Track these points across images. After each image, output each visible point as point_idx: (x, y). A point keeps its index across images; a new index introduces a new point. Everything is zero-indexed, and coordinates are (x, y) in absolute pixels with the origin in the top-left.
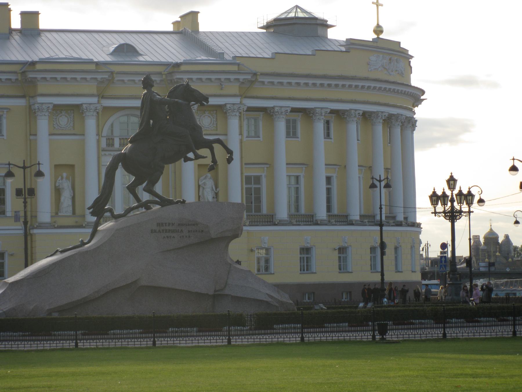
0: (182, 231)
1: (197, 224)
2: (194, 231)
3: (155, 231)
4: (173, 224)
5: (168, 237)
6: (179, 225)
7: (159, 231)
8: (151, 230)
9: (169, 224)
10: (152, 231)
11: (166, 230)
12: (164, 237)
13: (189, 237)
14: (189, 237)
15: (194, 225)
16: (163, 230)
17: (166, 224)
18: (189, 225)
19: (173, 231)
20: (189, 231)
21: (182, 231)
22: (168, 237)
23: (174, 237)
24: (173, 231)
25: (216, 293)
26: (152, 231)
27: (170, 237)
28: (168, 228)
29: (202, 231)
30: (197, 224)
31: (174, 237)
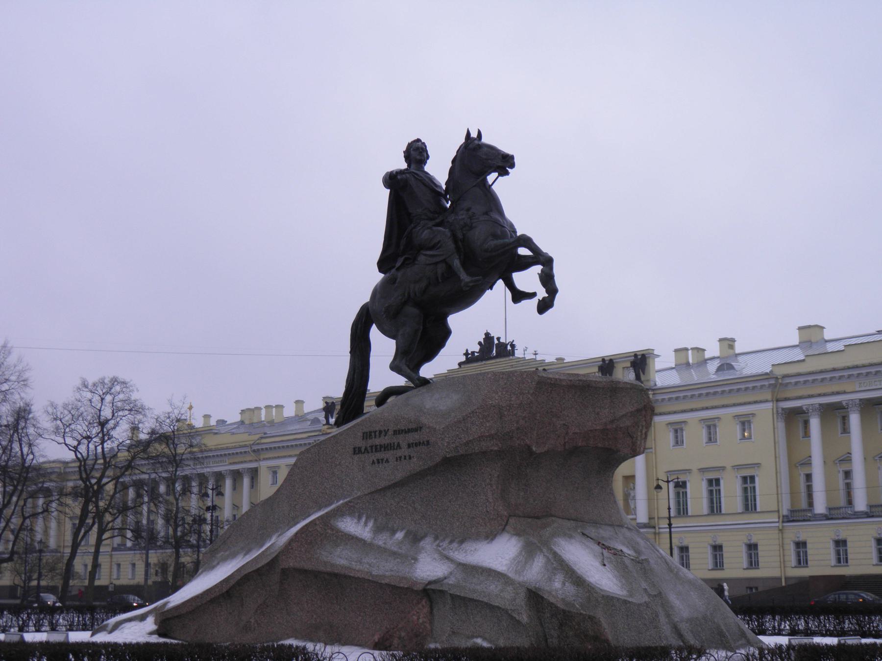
2: (416, 445)
4: (386, 432)
5: (379, 462)
6: (396, 432)
7: (366, 449)
8: (354, 448)
9: (380, 432)
10: (357, 451)
11: (376, 446)
12: (373, 462)
14: (410, 458)
15: (416, 430)
16: (372, 447)
17: (375, 432)
18: (409, 431)
20: (409, 446)
21: (399, 445)
23: (387, 461)
25: (428, 587)
26: (357, 451)
27: (382, 460)
28: (377, 441)
31: (387, 461)
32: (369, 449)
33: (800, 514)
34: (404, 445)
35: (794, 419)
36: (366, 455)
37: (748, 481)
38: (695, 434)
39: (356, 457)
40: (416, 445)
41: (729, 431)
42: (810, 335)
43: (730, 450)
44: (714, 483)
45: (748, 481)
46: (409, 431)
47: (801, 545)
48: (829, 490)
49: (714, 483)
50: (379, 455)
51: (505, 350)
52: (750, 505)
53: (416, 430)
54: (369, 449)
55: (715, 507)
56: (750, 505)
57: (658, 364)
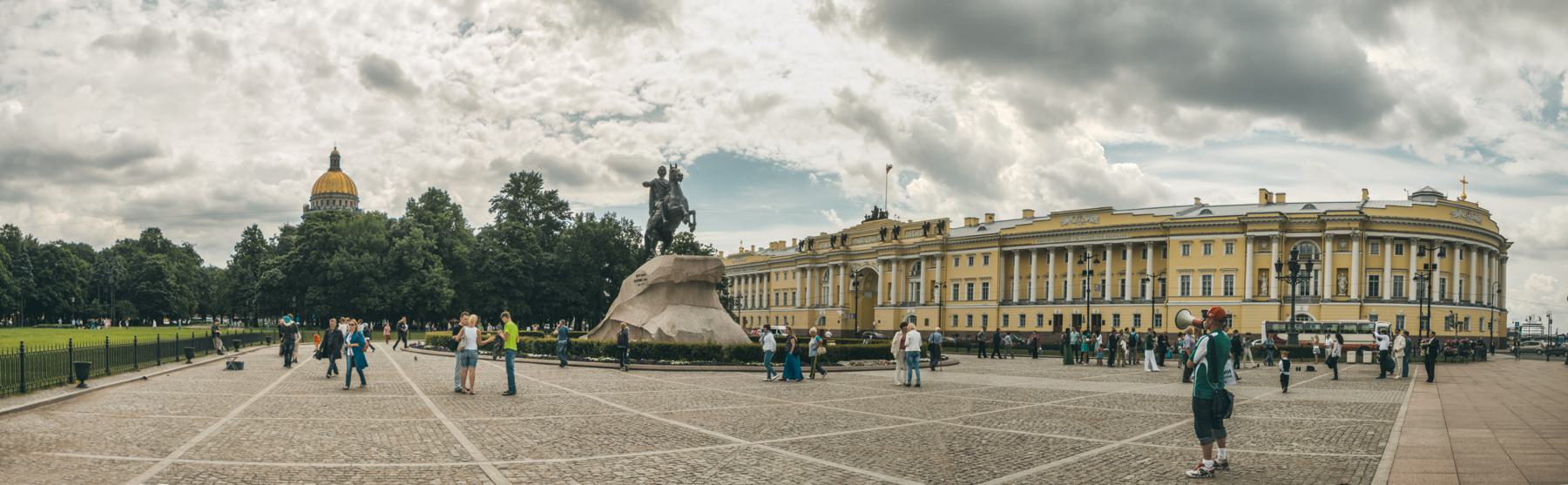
33: (1006, 301)
35: (1008, 256)
37: (986, 285)
38: (964, 261)
41: (979, 260)
42: (1028, 213)
43: (979, 271)
44: (971, 285)
45: (986, 285)
47: (1006, 316)
48: (1038, 288)
49: (971, 285)
51: (884, 215)
52: (985, 297)
55: (970, 298)
56: (985, 297)
57: (952, 226)
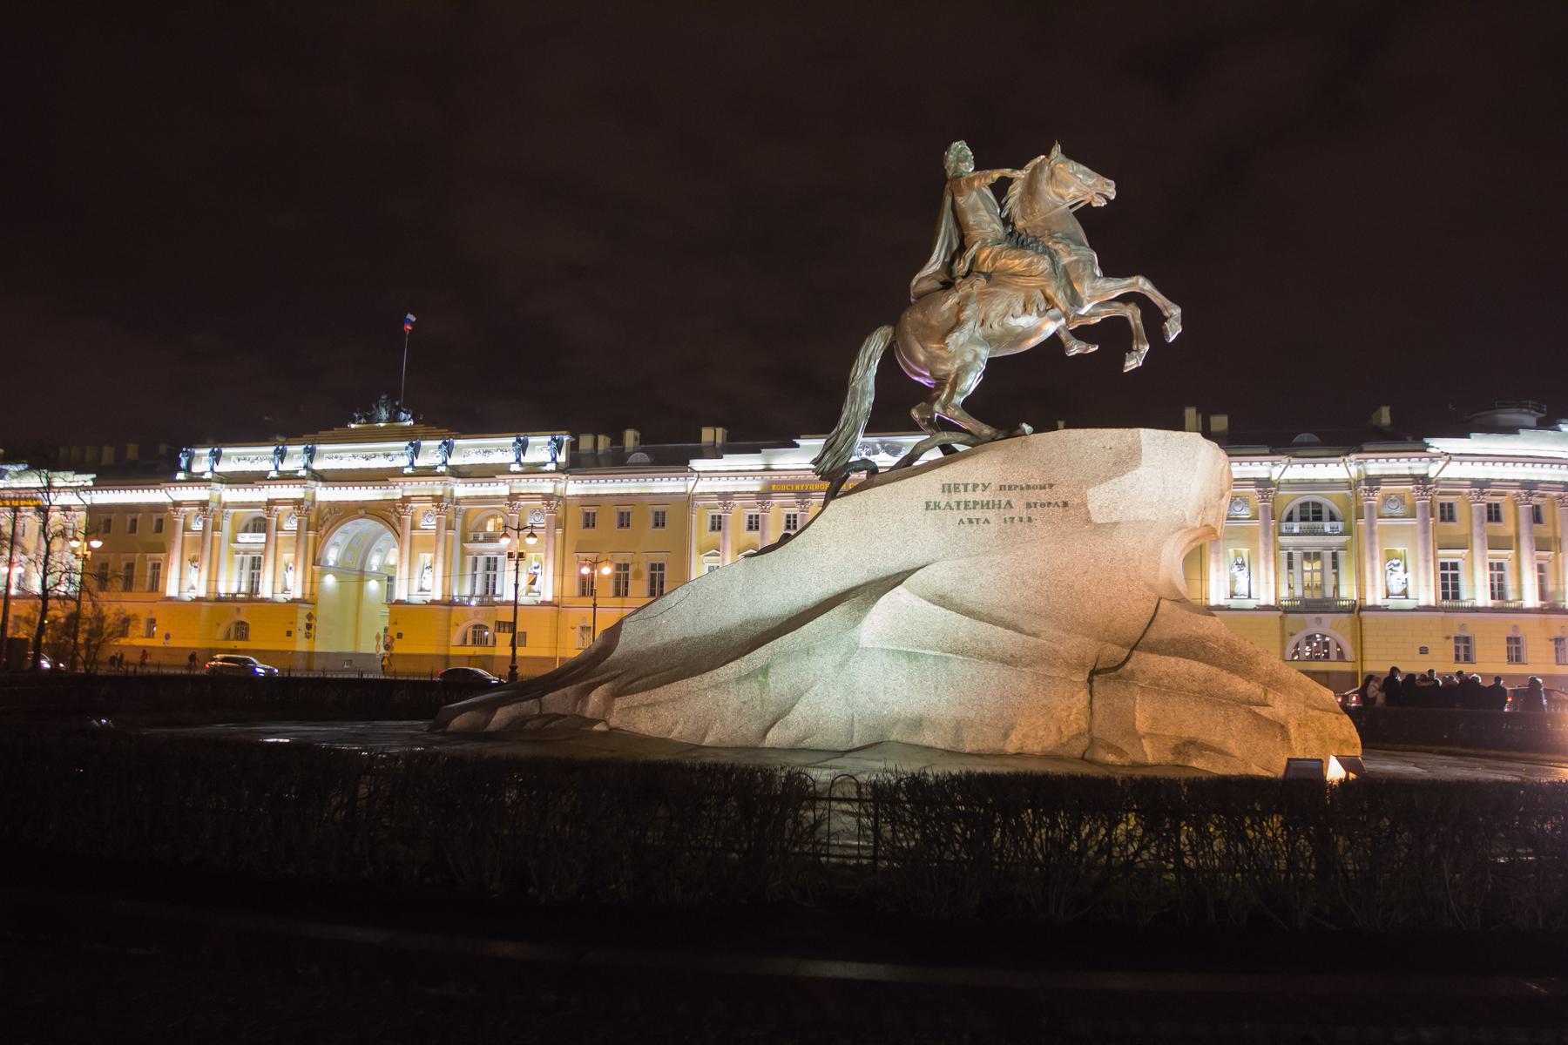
0: (1009, 503)
1: (1051, 486)
2: (1043, 505)
3: (937, 506)
4: (985, 487)
5: (970, 521)
6: (1002, 488)
7: (948, 504)
8: (928, 504)
9: (975, 486)
13: (1030, 520)
14: (1030, 520)
15: (1043, 487)
16: (958, 503)
17: (966, 486)
18: (1028, 487)
19: (986, 505)
21: (1009, 503)
22: (970, 521)
24: (986, 505)
28: (971, 496)
29: (1065, 504)
30: (1051, 486)
32: (954, 505)
34: (1019, 505)
36: (948, 512)
39: (931, 513)
40: (1043, 505)
46: (1028, 487)
50: (978, 513)
53: (1043, 487)
54: (954, 505)
